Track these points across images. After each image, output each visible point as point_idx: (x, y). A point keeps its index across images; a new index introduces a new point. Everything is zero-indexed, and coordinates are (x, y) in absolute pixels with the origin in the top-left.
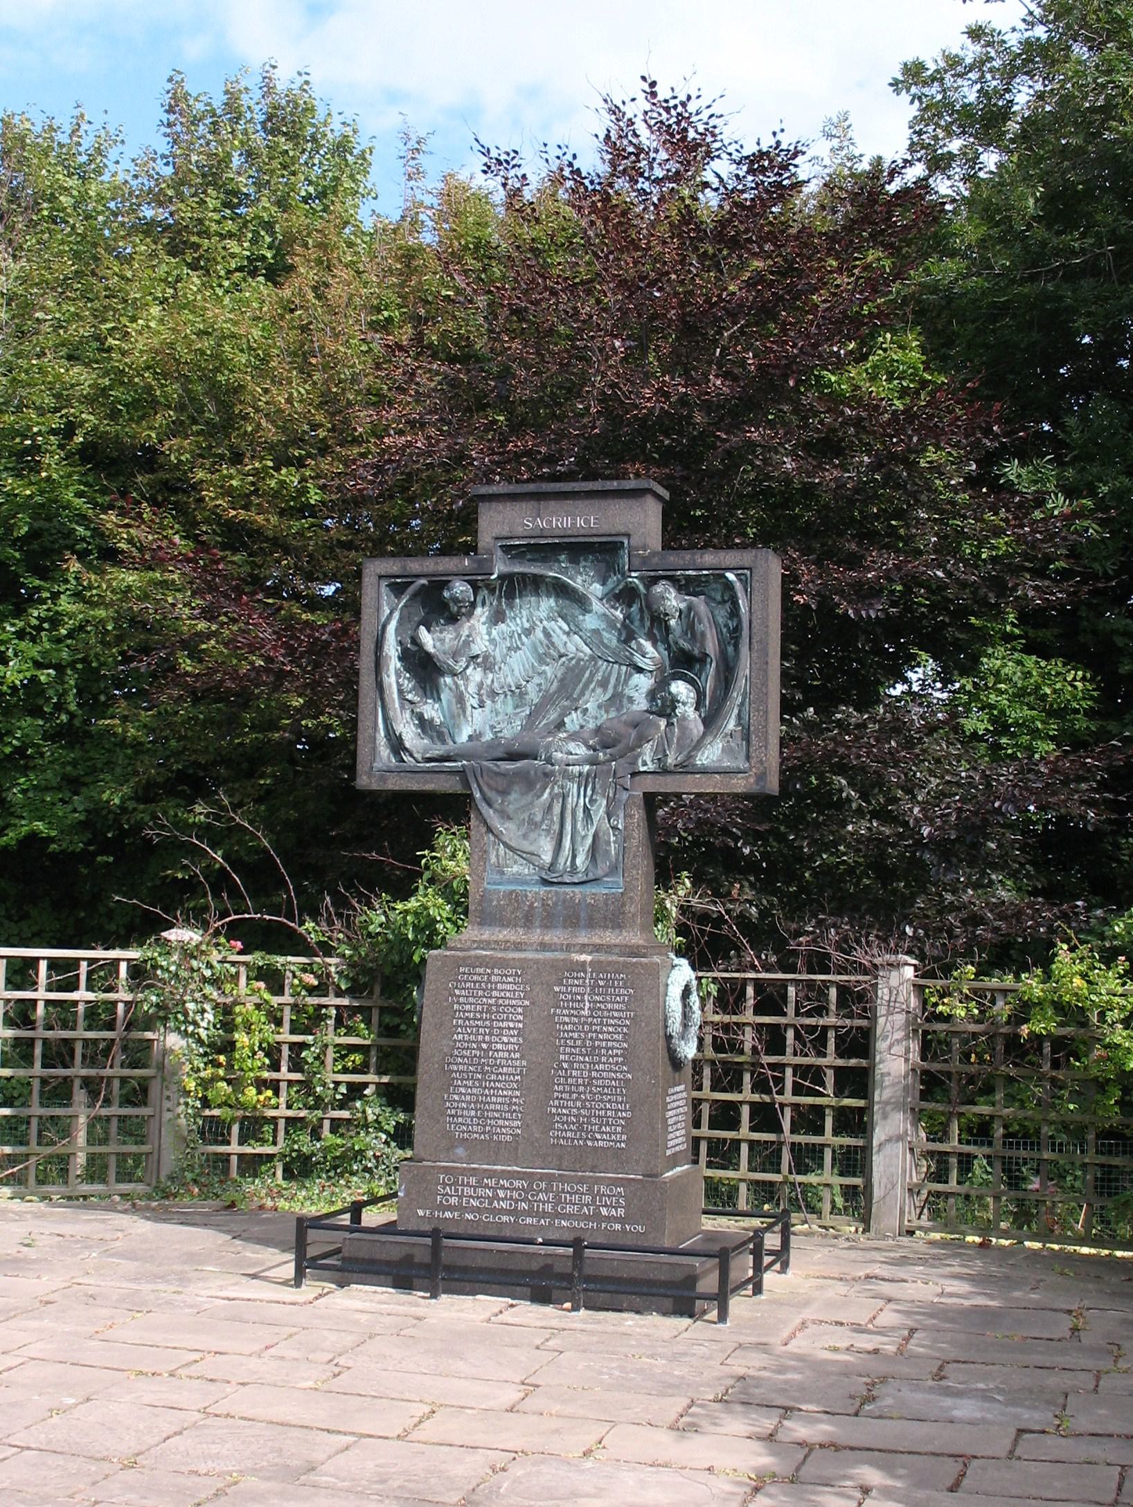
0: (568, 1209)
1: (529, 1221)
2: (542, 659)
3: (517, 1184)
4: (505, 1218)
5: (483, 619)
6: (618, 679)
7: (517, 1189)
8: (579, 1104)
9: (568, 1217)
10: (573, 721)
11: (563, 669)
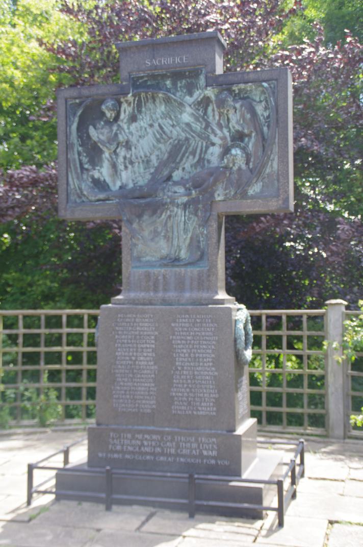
0: (184, 452)
1: (162, 458)
2: (158, 141)
3: (154, 437)
4: (148, 457)
5: (125, 121)
6: (201, 150)
7: (154, 440)
8: (188, 390)
9: (183, 456)
10: (177, 175)
11: (170, 146)
